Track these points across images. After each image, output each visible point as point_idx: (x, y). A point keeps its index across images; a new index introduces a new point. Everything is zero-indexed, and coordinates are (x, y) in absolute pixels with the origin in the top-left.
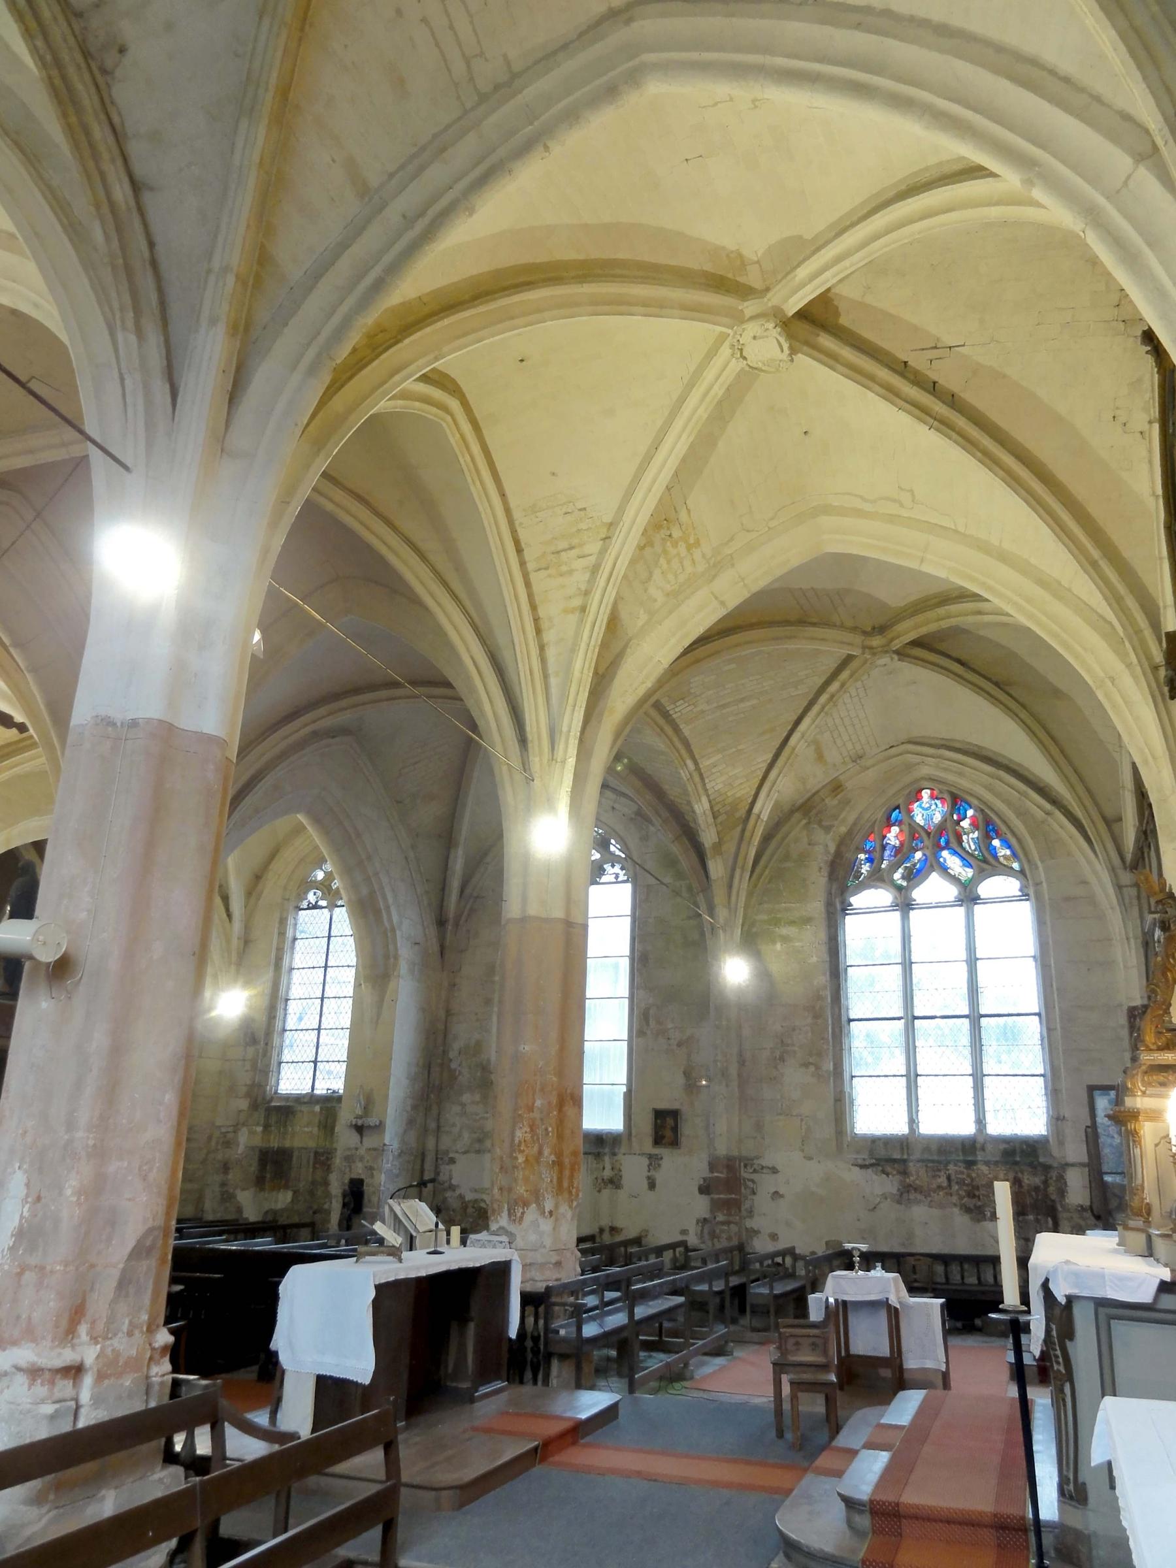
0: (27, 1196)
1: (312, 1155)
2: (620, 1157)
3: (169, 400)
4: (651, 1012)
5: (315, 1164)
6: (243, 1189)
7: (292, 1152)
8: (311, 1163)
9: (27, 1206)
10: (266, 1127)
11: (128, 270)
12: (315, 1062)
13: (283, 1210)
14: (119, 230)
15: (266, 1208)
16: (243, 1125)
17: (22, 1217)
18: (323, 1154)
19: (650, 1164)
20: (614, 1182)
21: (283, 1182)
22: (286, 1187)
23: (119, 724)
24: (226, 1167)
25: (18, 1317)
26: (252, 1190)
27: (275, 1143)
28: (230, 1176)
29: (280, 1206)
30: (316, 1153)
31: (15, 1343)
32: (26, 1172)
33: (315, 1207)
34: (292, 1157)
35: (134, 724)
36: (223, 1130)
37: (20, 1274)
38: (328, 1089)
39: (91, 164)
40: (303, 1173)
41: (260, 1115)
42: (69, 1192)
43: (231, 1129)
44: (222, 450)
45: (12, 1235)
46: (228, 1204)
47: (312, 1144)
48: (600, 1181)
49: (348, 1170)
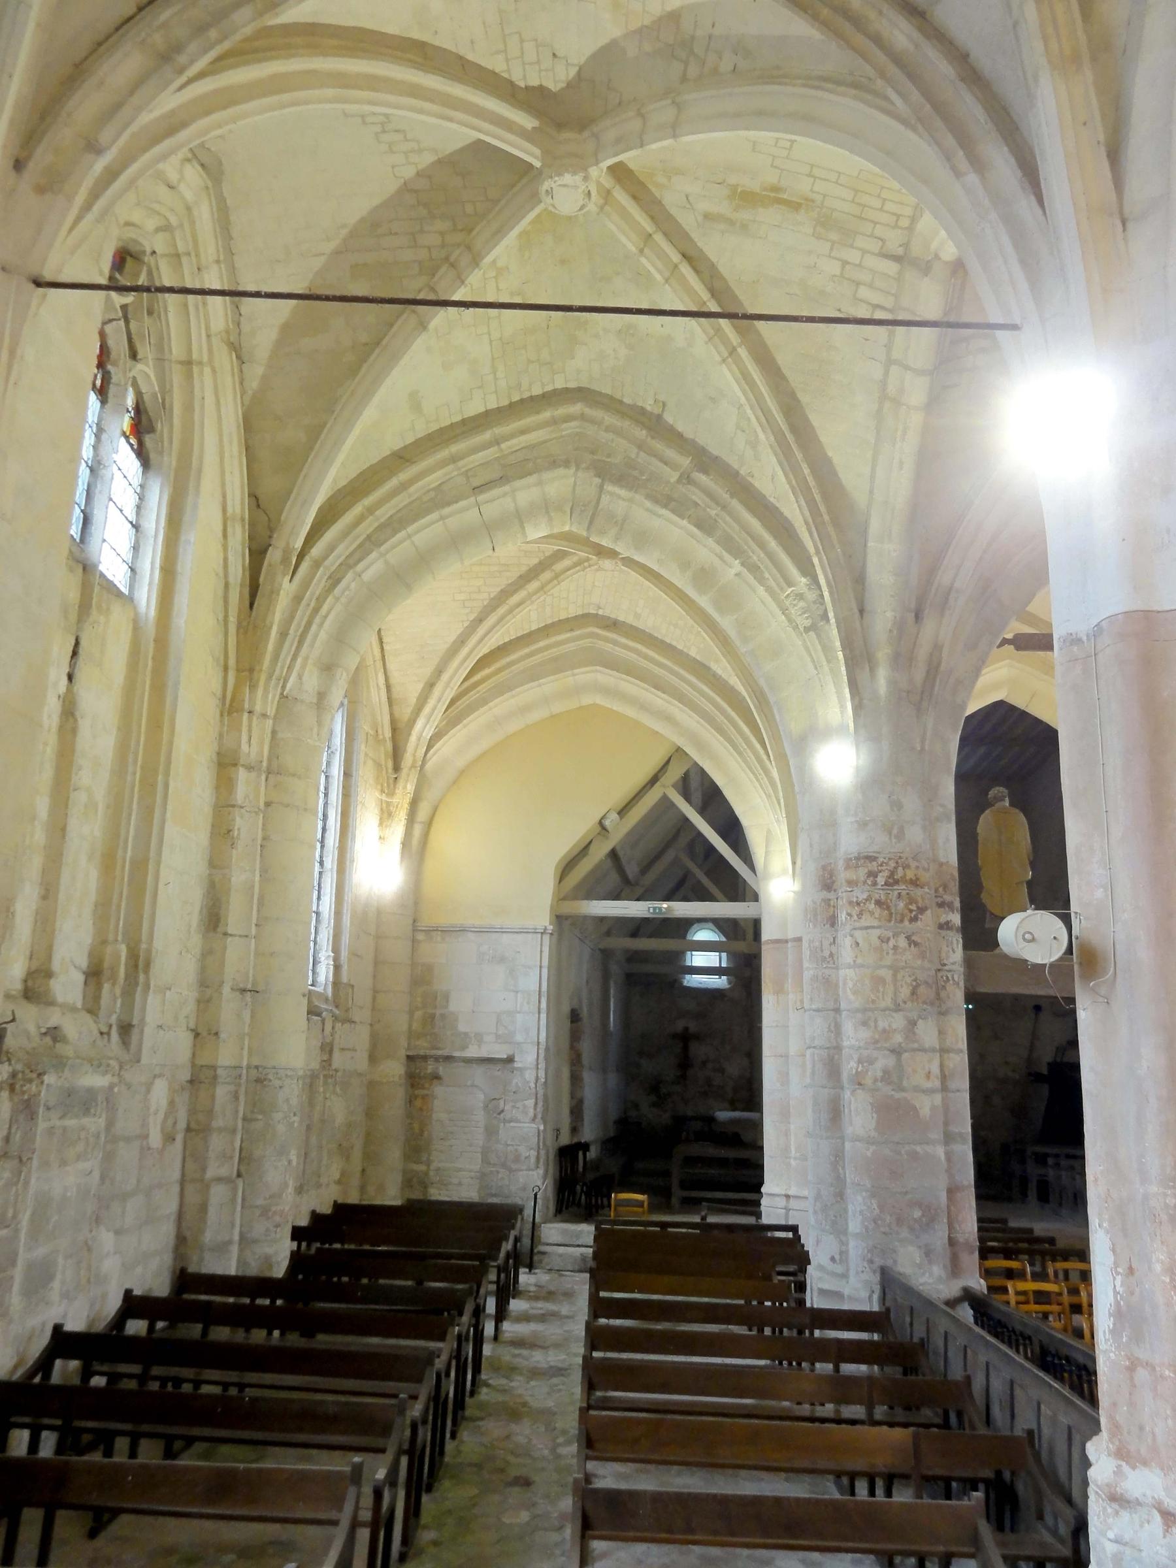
0: (1116, 1265)
3: (1040, 212)
9: (1119, 1278)
11: (940, 108)
14: (913, 76)
17: (1116, 1293)
23: (1085, 638)
25: (1141, 1428)
31: (1145, 1463)
32: (1107, 1232)
35: (1098, 631)
37: (1131, 1369)
39: (859, 39)
42: (1158, 1268)
44: (1124, 223)
45: (1110, 1315)
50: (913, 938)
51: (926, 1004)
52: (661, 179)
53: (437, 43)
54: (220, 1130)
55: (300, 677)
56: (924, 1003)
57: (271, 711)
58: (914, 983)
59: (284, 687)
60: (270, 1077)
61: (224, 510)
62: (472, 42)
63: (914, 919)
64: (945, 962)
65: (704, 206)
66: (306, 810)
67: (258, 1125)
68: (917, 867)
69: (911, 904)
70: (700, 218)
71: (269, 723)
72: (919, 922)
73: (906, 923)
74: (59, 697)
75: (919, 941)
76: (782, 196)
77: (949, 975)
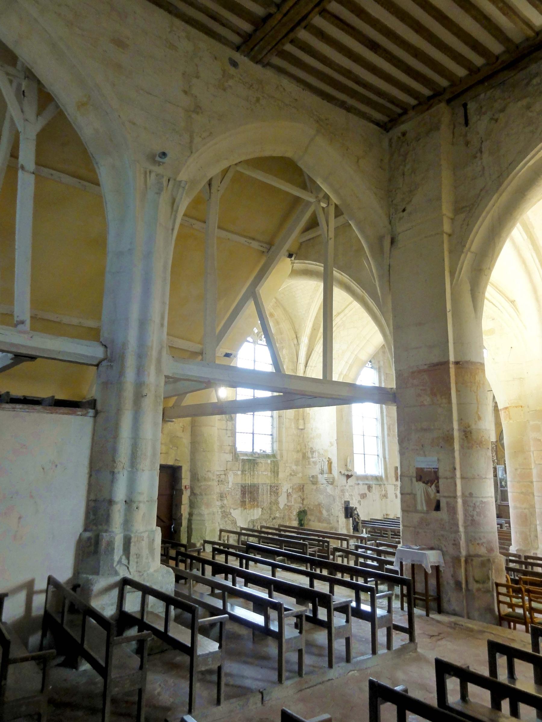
1: (269, 487)
2: (386, 485)
4: (391, 426)
5: (271, 492)
6: (234, 509)
7: (259, 486)
8: (269, 493)
10: (243, 471)
12: (253, 434)
13: (257, 520)
15: (249, 519)
16: (230, 470)
18: (274, 486)
19: (395, 489)
20: (385, 496)
21: (256, 503)
22: (258, 506)
24: (222, 497)
26: (240, 509)
27: (249, 482)
28: (225, 502)
29: (256, 517)
30: (271, 486)
33: (272, 516)
34: (259, 488)
36: (218, 473)
38: (260, 450)
40: (265, 497)
41: (239, 465)
43: (223, 473)
46: (226, 519)
47: (268, 482)
48: (382, 495)
49: (343, 497)
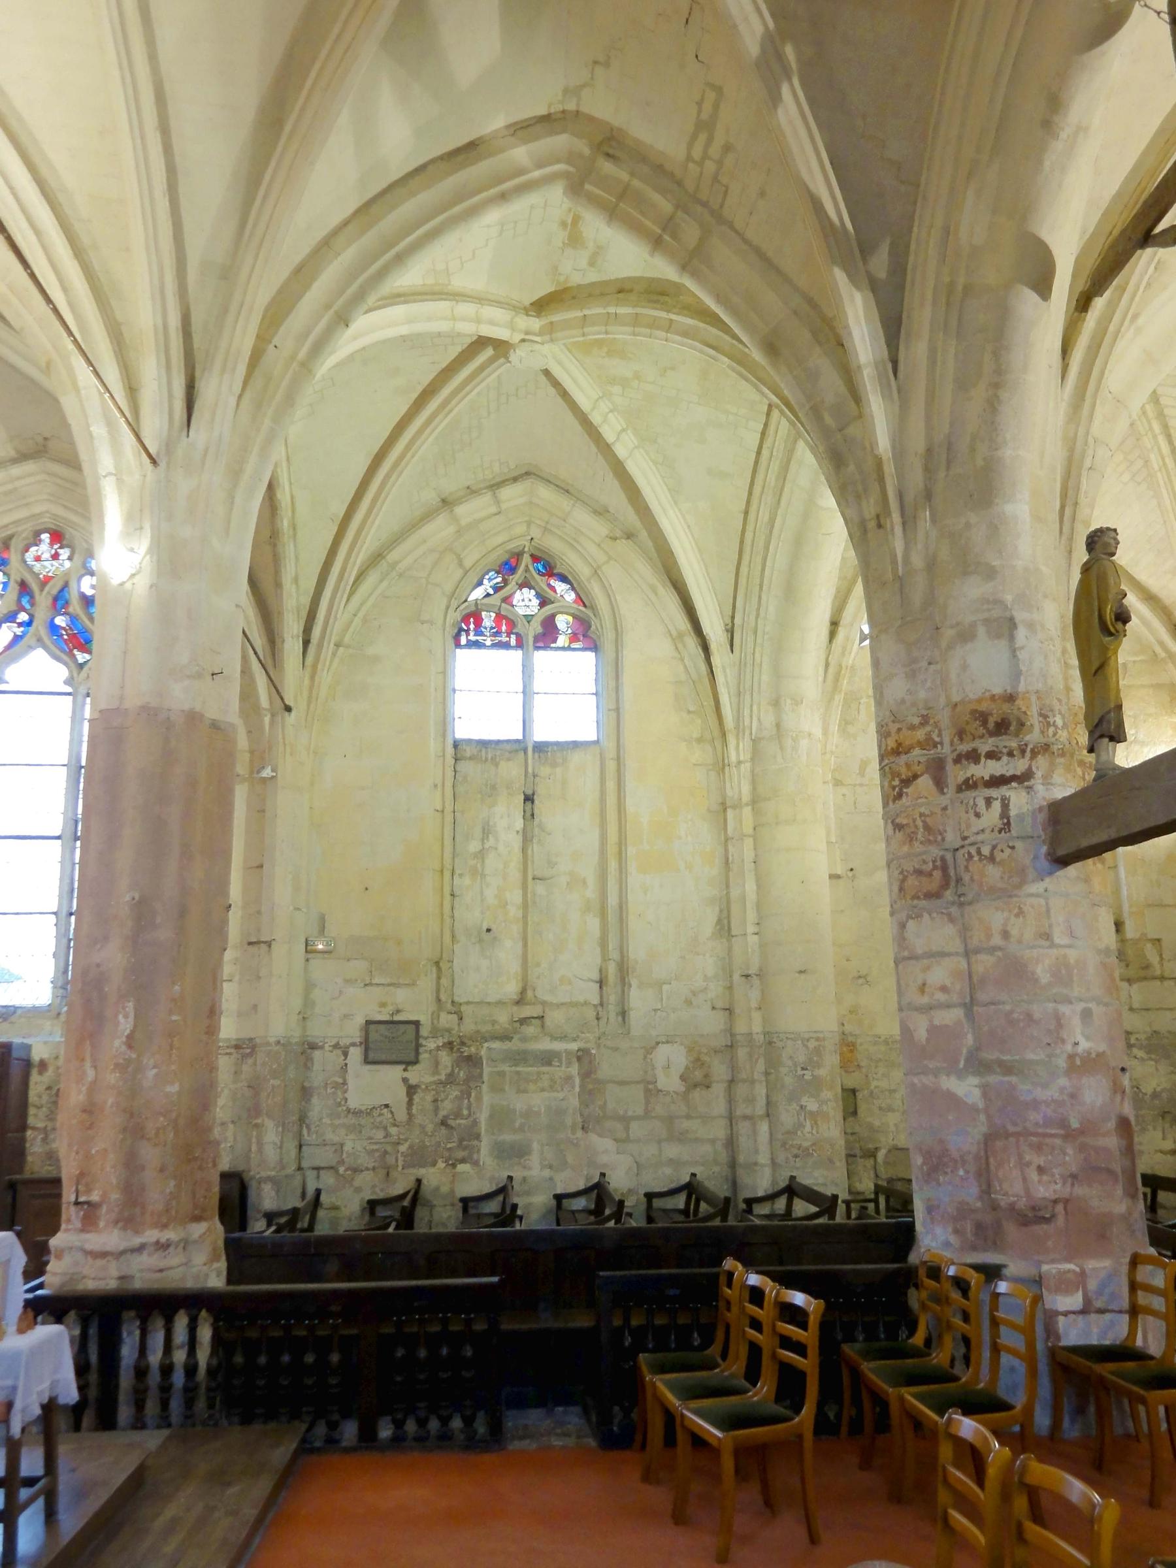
50: (898, 821)
51: (918, 898)
52: (562, 279)
53: (426, 384)
54: (744, 1081)
55: (759, 719)
56: (915, 897)
57: (745, 755)
58: (901, 877)
59: (751, 734)
60: (775, 1040)
61: (671, 635)
62: (433, 363)
63: (900, 796)
64: (966, 834)
65: (583, 263)
66: (777, 824)
67: (772, 1077)
68: (899, 730)
69: (893, 779)
70: (593, 269)
71: (748, 765)
72: (904, 799)
73: (891, 803)
74: (518, 832)
75: (905, 822)
76: (569, 221)
77: (973, 850)
